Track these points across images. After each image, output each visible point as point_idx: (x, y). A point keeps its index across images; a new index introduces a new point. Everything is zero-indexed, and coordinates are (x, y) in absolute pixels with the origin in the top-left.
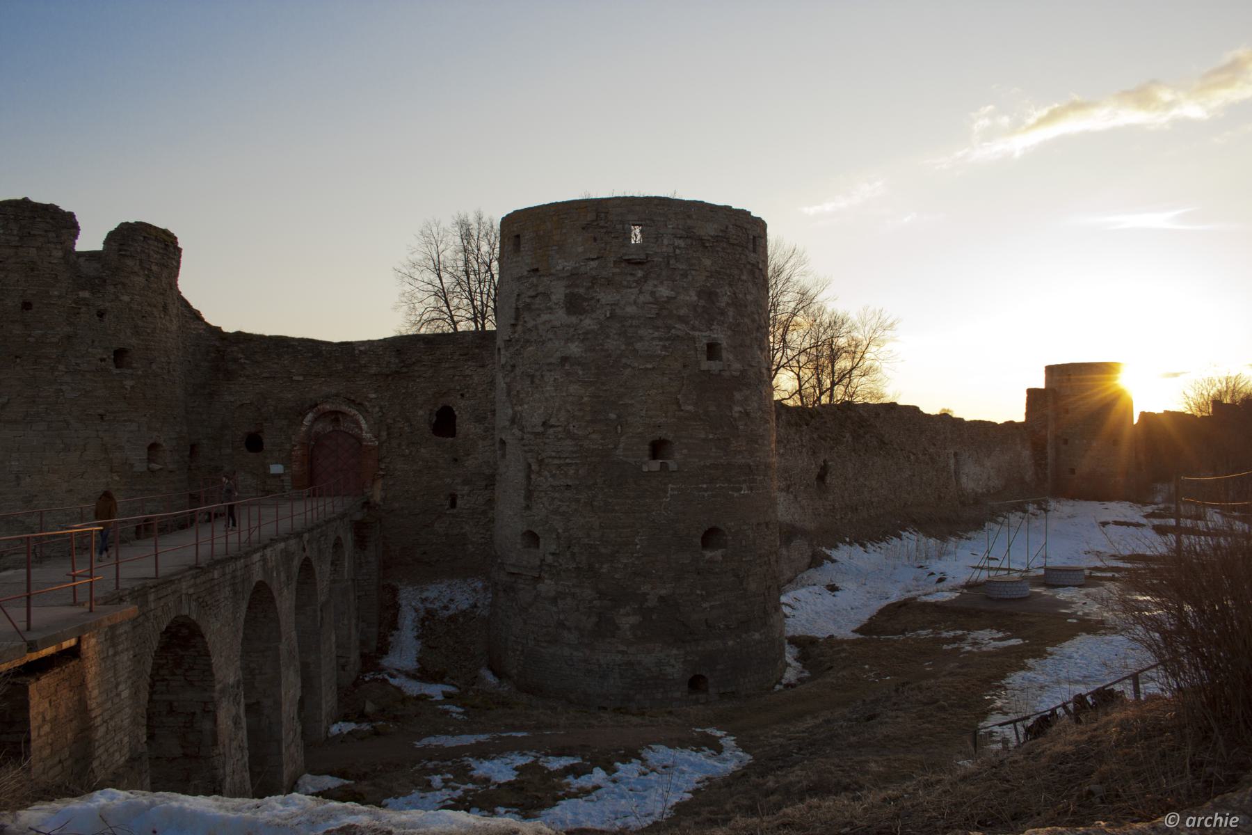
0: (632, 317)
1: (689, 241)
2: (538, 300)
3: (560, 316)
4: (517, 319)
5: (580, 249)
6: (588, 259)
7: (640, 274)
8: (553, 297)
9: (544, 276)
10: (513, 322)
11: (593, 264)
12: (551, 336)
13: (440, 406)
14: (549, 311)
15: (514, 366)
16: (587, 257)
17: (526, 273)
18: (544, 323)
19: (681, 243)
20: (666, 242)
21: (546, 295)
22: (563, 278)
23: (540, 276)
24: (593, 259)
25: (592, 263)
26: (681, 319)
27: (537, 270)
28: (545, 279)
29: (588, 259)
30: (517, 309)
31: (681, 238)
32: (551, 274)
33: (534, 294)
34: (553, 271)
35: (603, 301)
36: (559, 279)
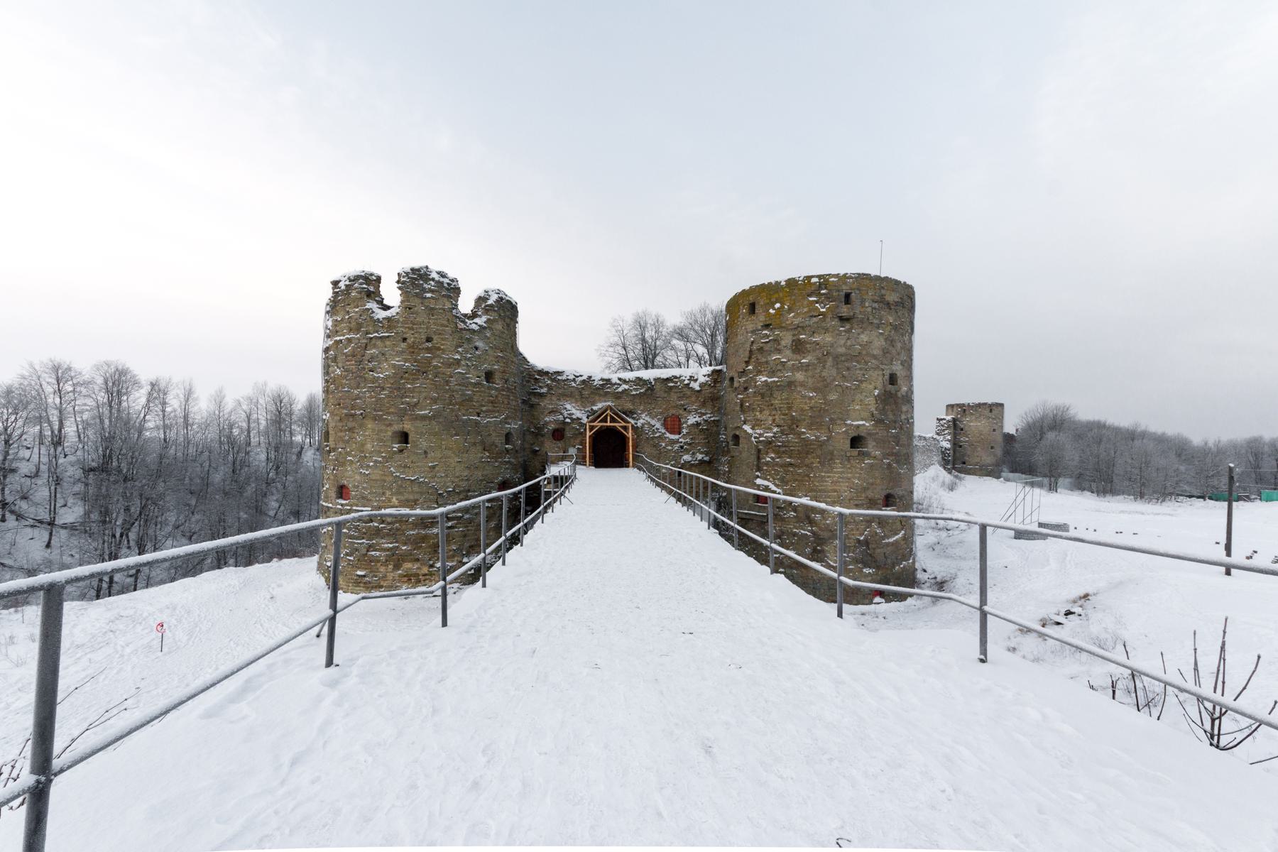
0: (842, 355)
1: (881, 305)
2: (769, 345)
4: (750, 358)
5: (806, 310)
6: (812, 316)
8: (783, 343)
10: (747, 359)
12: (779, 367)
15: (746, 389)
16: (811, 315)
17: (760, 327)
19: (876, 305)
20: (867, 304)
23: (772, 329)
24: (815, 316)
25: (814, 319)
26: (875, 357)
29: (812, 316)
30: (751, 351)
31: (876, 302)
34: (784, 325)
36: (788, 330)
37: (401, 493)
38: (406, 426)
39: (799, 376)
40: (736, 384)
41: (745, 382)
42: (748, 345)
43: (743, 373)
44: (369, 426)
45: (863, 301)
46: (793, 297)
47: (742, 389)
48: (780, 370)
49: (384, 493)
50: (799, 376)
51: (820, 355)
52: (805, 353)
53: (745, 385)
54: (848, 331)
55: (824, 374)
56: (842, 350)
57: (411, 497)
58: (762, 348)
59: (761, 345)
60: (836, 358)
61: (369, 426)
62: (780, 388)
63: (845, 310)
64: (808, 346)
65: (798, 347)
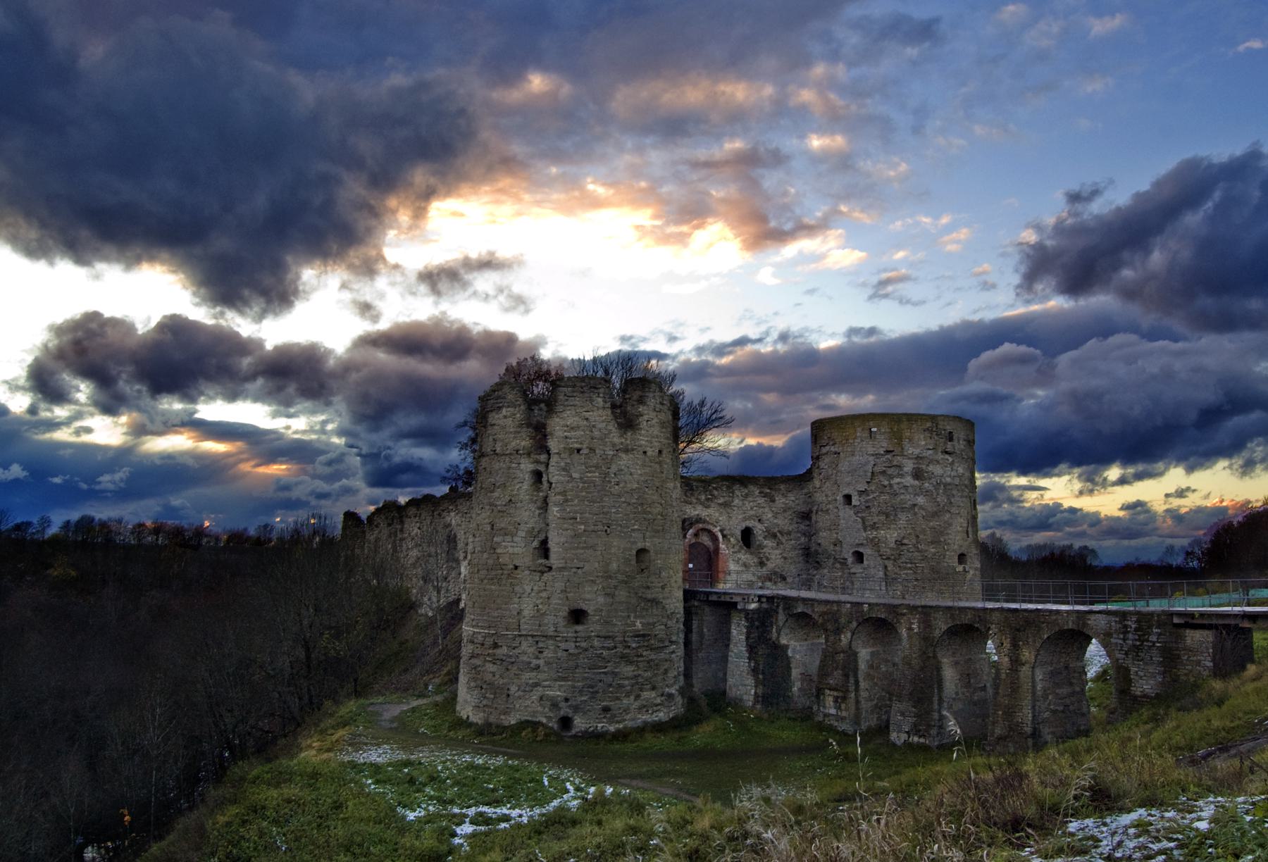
0: (949, 484)
2: (892, 469)
3: (909, 480)
5: (923, 443)
7: (951, 459)
8: (905, 469)
11: (930, 452)
12: (902, 491)
13: (744, 526)
18: (898, 483)
21: (899, 467)
22: (912, 459)
28: (899, 458)
34: (905, 453)
35: (935, 473)
36: (909, 458)
37: (643, 617)
38: (647, 544)
39: (921, 500)
40: (855, 501)
42: (869, 468)
43: (861, 493)
45: (959, 441)
47: (863, 507)
49: (629, 616)
50: (921, 500)
51: (935, 483)
54: (952, 463)
55: (938, 500)
56: (948, 480)
57: (651, 621)
58: (884, 472)
60: (946, 485)
63: (949, 447)
65: (918, 475)
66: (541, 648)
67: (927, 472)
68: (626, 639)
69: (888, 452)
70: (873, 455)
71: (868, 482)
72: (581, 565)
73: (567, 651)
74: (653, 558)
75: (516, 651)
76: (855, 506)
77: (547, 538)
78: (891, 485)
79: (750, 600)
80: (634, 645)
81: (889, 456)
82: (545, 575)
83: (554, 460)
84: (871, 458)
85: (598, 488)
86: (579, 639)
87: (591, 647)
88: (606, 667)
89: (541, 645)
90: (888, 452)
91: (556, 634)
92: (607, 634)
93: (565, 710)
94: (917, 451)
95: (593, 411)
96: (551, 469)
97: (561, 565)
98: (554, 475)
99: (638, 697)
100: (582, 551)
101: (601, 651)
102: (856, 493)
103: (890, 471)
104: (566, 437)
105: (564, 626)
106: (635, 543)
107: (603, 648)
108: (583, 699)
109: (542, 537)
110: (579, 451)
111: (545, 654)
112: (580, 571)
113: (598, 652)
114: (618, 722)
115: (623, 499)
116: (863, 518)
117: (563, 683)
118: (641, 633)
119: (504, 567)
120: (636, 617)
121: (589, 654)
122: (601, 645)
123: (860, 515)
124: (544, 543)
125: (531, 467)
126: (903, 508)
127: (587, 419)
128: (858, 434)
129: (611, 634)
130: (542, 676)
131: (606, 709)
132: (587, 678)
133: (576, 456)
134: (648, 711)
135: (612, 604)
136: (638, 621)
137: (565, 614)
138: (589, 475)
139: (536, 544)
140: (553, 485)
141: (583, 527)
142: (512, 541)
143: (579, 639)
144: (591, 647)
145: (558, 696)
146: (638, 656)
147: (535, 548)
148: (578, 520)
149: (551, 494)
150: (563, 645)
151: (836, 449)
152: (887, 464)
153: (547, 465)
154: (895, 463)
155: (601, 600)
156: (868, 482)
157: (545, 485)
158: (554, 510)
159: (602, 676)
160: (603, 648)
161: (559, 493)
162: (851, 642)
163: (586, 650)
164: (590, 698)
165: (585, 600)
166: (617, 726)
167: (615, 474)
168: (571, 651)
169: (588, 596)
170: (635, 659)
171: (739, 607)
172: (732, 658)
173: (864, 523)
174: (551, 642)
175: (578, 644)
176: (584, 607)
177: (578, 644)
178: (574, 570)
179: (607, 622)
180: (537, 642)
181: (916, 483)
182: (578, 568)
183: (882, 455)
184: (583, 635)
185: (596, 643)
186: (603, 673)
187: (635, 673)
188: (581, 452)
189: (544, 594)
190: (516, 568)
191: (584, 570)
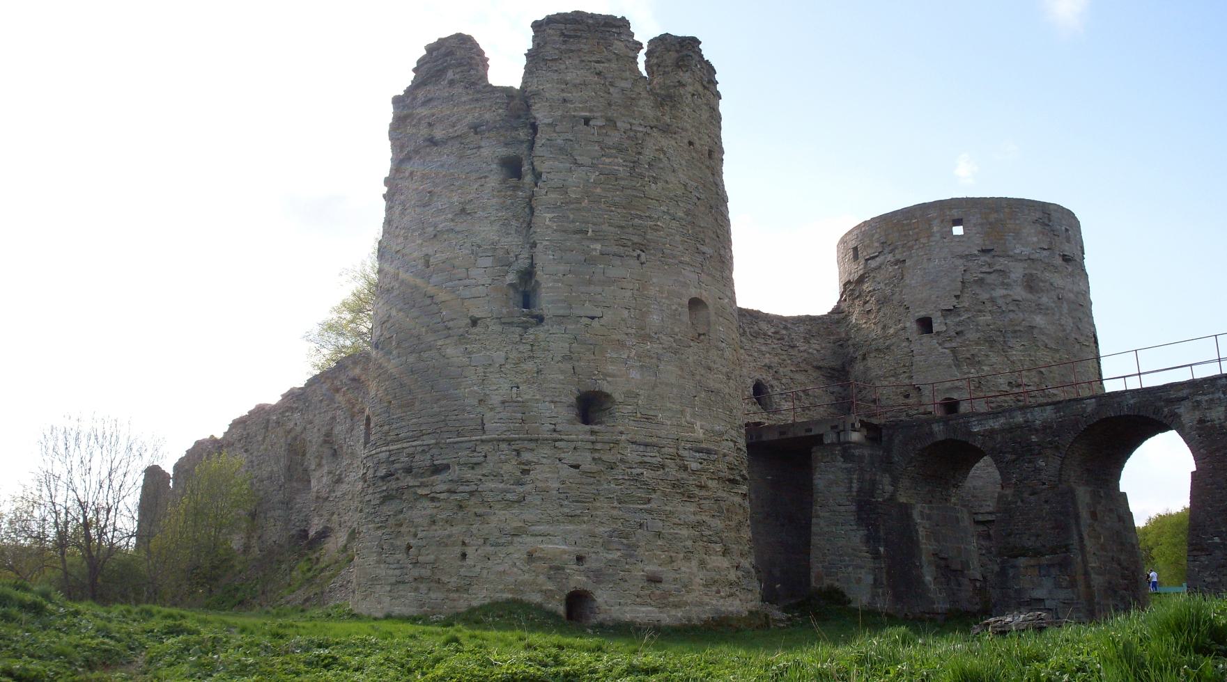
2: (993, 276)
3: (1019, 292)
8: (1013, 276)
9: (999, 256)
10: (959, 293)
11: (1045, 253)
14: (1006, 287)
17: (976, 252)
18: (1005, 296)
22: (1021, 260)
23: (994, 256)
24: (1045, 249)
27: (989, 251)
32: (1008, 256)
33: (991, 270)
34: (1011, 253)
36: (1016, 260)
39: (1039, 320)
41: (958, 324)
43: (947, 312)
44: (655, 280)
46: (1017, 222)
47: (953, 334)
48: (1013, 311)
49: (682, 412)
52: (1037, 292)
53: (959, 329)
56: (1071, 295)
59: (982, 275)
61: (655, 280)
62: (1019, 334)
64: (1041, 284)
65: (1031, 284)
66: (528, 463)
67: (1042, 281)
68: (681, 452)
69: (984, 251)
70: (961, 257)
71: (957, 297)
72: (598, 312)
73: (576, 467)
74: (713, 318)
75: (479, 471)
76: (938, 333)
77: (532, 265)
78: (992, 300)
79: (849, 427)
80: (694, 466)
81: (986, 258)
82: (531, 331)
83: (541, 139)
84: (959, 262)
85: (622, 183)
86: (598, 446)
87: (621, 460)
88: (649, 501)
89: (526, 456)
90: (984, 251)
91: (555, 436)
92: (649, 440)
93: (577, 580)
94: (1027, 251)
95: (609, 60)
96: (538, 150)
97: (561, 312)
98: (546, 163)
99: (702, 563)
100: (599, 289)
101: (639, 471)
102: (939, 313)
103: (990, 279)
104: (565, 101)
105: (570, 422)
106: (685, 285)
107: (642, 464)
108: (610, 557)
109: (523, 263)
110: (587, 121)
111: (532, 475)
112: (595, 323)
113: (635, 471)
114: (676, 606)
115: (664, 208)
116: (953, 350)
117: (571, 527)
118: (704, 445)
119: (451, 324)
120: (694, 415)
121: (618, 473)
122: (639, 459)
123: (947, 345)
124: (528, 275)
125: (503, 151)
126: (1015, 332)
127: (599, 74)
128: (935, 229)
129: (655, 440)
130: (529, 515)
131: (654, 580)
132: (615, 519)
133: (582, 127)
134: (718, 592)
135: (655, 386)
136: (698, 424)
137: (573, 399)
138: (607, 160)
139: (511, 278)
140: (544, 176)
141: (598, 246)
142: (468, 277)
143: (598, 446)
144: (621, 460)
145: (564, 552)
146: (701, 487)
147: (511, 285)
148: (589, 234)
149: (540, 192)
150: (570, 457)
151: (898, 257)
152: (985, 269)
153: (532, 145)
154: (997, 267)
155: (635, 375)
156: (957, 297)
157: (528, 179)
158: (545, 218)
159: (646, 516)
160: (642, 464)
161: (555, 189)
162: (1060, 470)
163: (612, 467)
164: (625, 556)
165: (606, 375)
166: (673, 612)
167: (649, 164)
168: (584, 467)
169: (611, 368)
170: (697, 491)
171: (827, 441)
172: (820, 524)
173: (956, 358)
174: (546, 451)
175: (597, 455)
176: (607, 388)
177: (597, 455)
178: (588, 321)
179: (648, 419)
180: (518, 453)
181: (1030, 296)
182: (593, 318)
183: (976, 256)
184: (606, 438)
185: (631, 454)
186: (646, 510)
187: (698, 517)
188: (591, 123)
189: (529, 366)
190: (474, 322)
191: (603, 321)
